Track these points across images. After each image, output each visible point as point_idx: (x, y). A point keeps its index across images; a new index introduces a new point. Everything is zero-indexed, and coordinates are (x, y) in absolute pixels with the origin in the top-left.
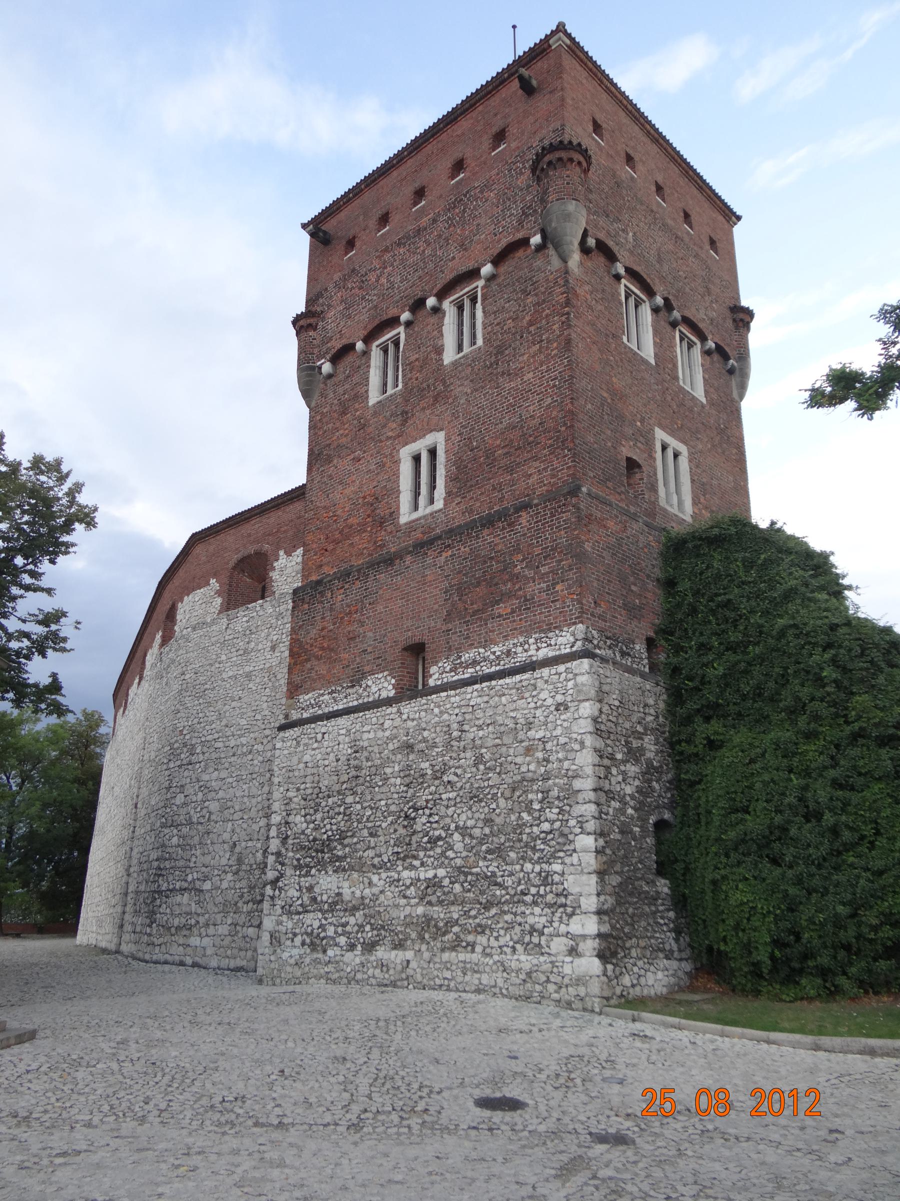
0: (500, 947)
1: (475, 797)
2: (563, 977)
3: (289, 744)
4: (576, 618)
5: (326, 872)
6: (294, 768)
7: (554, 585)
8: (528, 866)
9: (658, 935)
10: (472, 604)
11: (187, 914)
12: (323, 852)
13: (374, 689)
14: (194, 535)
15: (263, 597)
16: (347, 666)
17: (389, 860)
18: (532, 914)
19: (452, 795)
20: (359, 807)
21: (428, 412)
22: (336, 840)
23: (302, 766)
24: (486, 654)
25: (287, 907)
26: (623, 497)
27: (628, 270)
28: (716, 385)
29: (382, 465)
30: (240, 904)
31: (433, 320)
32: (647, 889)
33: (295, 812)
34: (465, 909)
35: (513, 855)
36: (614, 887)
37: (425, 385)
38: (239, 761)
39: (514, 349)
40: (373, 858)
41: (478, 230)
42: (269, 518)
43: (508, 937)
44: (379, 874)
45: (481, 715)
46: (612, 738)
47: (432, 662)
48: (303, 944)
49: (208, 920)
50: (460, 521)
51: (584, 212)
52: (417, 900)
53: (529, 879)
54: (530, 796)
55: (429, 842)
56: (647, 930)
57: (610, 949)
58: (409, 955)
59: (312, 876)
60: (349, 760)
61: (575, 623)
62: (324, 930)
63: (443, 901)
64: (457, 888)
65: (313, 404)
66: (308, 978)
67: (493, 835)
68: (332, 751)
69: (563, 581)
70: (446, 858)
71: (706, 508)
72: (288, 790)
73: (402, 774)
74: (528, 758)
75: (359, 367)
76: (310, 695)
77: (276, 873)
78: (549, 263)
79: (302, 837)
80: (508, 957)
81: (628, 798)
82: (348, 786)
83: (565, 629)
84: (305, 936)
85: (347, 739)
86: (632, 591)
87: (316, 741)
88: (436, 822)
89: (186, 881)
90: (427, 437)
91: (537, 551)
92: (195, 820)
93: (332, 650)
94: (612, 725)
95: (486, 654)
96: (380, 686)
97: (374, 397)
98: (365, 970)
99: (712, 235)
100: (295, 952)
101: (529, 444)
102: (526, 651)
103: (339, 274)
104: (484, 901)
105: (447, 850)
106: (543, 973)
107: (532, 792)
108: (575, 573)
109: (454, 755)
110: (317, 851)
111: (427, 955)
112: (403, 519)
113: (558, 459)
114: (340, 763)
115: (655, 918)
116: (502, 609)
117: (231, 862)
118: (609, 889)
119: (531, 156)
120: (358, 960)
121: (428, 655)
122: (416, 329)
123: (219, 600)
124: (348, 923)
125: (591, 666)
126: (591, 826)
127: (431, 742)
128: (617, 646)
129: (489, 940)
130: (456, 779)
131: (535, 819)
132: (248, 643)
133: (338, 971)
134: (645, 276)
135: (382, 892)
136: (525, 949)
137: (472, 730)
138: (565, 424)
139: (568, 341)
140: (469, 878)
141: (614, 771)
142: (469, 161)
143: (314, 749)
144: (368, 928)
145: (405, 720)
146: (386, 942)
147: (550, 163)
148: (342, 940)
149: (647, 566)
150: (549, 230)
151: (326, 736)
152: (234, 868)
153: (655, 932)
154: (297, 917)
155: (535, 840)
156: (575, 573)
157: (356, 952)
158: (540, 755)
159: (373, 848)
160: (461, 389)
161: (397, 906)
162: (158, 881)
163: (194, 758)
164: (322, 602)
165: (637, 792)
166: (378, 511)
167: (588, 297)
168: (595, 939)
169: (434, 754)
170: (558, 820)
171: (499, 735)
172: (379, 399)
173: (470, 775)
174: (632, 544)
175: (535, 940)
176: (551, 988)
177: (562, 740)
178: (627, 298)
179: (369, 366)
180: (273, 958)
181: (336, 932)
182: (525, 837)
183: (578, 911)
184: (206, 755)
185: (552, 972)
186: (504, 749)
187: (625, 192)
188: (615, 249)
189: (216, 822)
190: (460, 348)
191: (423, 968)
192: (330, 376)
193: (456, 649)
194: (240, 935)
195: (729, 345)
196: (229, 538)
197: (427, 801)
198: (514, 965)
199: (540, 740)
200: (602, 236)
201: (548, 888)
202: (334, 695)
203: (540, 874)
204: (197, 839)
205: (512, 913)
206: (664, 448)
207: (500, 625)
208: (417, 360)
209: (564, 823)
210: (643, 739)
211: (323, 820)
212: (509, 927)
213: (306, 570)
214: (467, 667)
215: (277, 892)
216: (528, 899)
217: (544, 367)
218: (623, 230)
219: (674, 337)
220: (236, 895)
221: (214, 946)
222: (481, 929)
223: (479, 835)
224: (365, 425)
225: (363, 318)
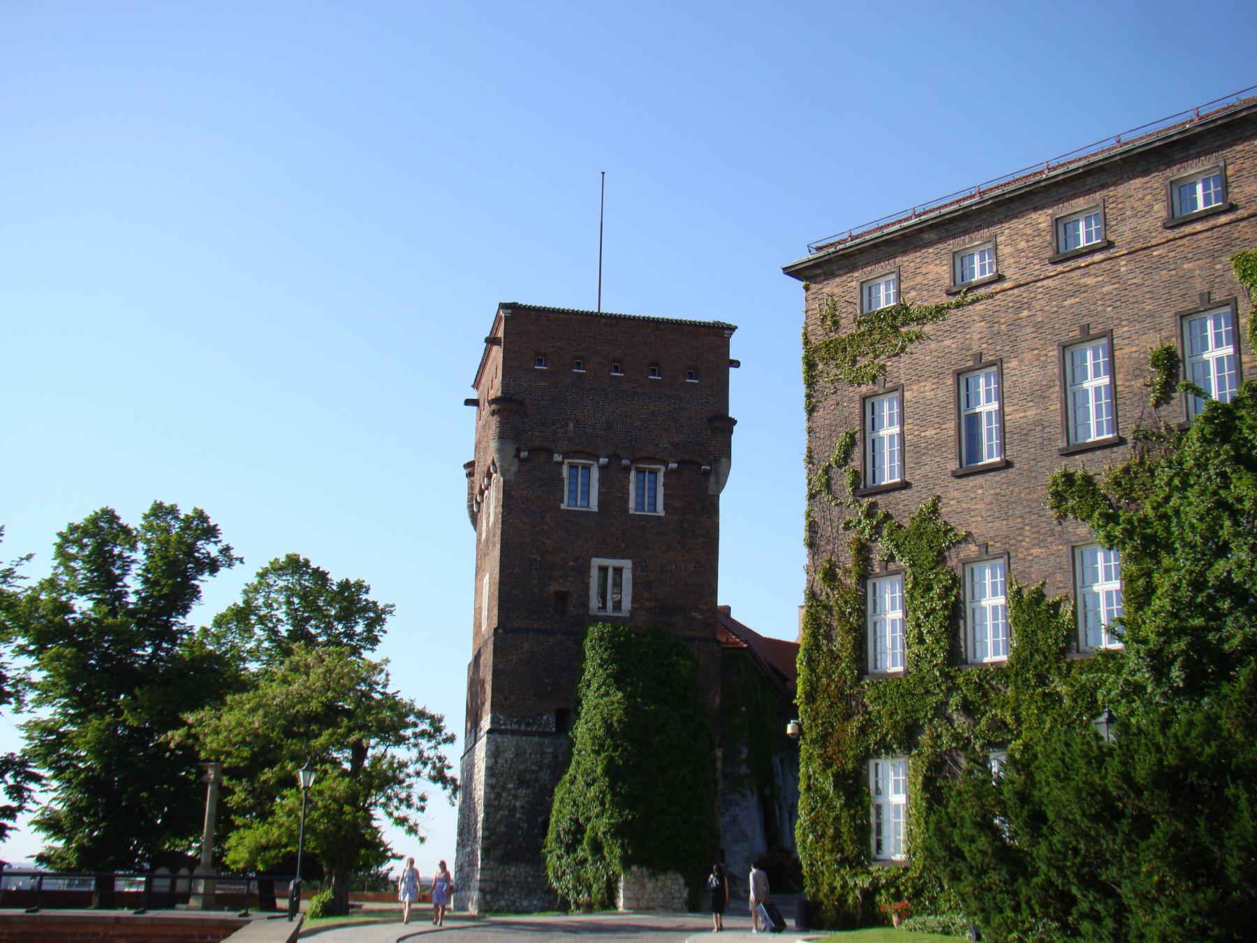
141: (504, 795)
200: (537, 443)
219: (628, 478)
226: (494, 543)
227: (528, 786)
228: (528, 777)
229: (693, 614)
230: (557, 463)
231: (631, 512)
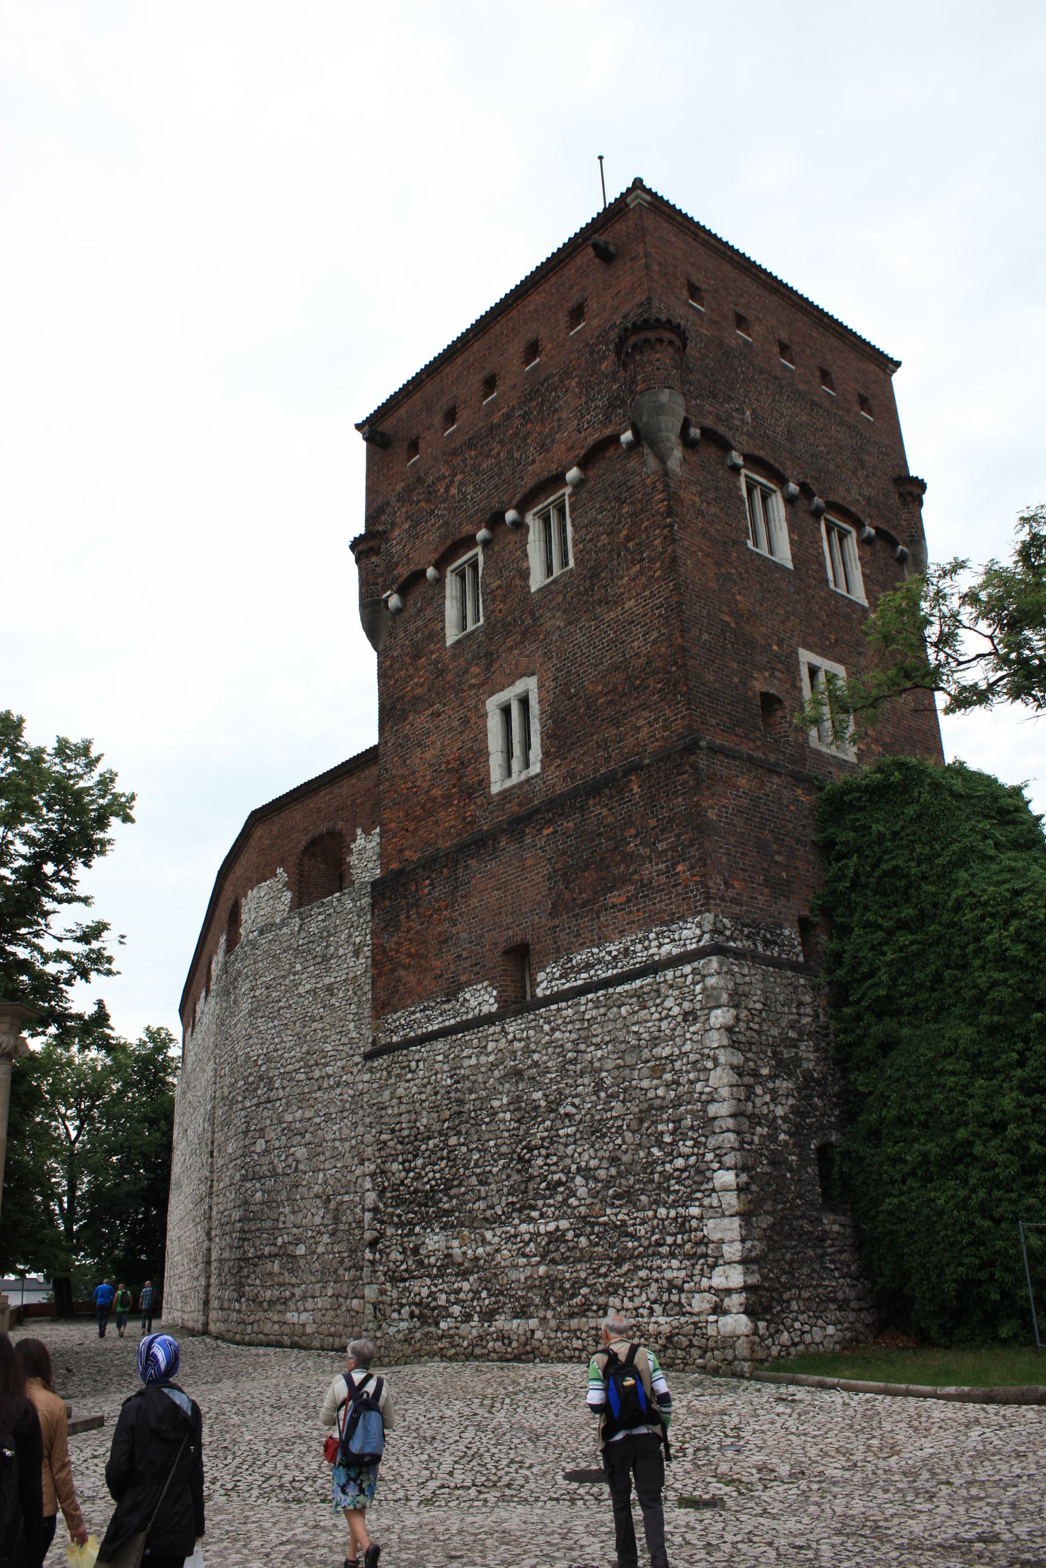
0: (636, 1309)
1: (596, 1131)
2: (708, 1340)
3: (378, 1075)
4: (701, 906)
5: (433, 1230)
6: (387, 1104)
7: (674, 865)
8: (662, 1212)
9: (827, 1283)
10: (581, 893)
11: (281, 1285)
12: (426, 1206)
13: (473, 1003)
14: (254, 814)
15: (340, 890)
16: (441, 976)
17: (503, 1212)
18: (670, 1268)
19: (571, 1130)
20: (464, 1149)
21: (516, 652)
22: (441, 1191)
23: (395, 1101)
24: (601, 955)
25: (390, 1273)
26: (759, 743)
27: (746, 457)
28: (881, 579)
29: (465, 722)
30: (340, 1272)
31: (514, 537)
32: (810, 1229)
33: (391, 1158)
34: (594, 1266)
35: (643, 1198)
36: (765, 1230)
37: (509, 619)
38: (326, 1097)
39: (611, 571)
40: (484, 1210)
41: (559, 426)
42: (341, 787)
43: (644, 1297)
44: (493, 1229)
45: (599, 1030)
46: (754, 1050)
47: (539, 968)
48: (412, 1315)
49: (305, 1292)
50: (561, 788)
51: (680, 400)
52: (538, 1259)
53: (664, 1227)
54: (660, 1127)
55: (547, 1188)
56: (813, 1278)
57: (761, 1303)
58: (533, 1323)
59: (416, 1235)
60: (449, 1093)
61: (700, 913)
62: (435, 1299)
63: (568, 1258)
64: (583, 1241)
65: (381, 647)
66: (421, 1356)
67: (621, 1177)
68: (429, 1083)
69: (683, 861)
70: (569, 1206)
71: (876, 741)
72: (381, 1132)
73: (512, 1108)
74: (655, 1082)
75: (432, 598)
76: (399, 1014)
77: (375, 1233)
78: (644, 463)
79: (402, 1188)
80: (645, 1320)
81: (780, 1122)
82: (451, 1125)
83: (690, 920)
84: (413, 1307)
85: (446, 1067)
86: (776, 862)
87: (410, 1071)
88: (555, 1164)
89: (275, 1245)
90: (517, 683)
91: (653, 822)
92: (280, 1170)
93: (420, 956)
94: (754, 1034)
95: (601, 955)
96: (480, 1000)
97: (452, 635)
98: (484, 1343)
99: (862, 392)
100: (404, 1325)
101: (636, 689)
102: (647, 949)
103: (402, 484)
104: (615, 1256)
105: (569, 1197)
106: (685, 1336)
107: (662, 1122)
108: (698, 849)
109: (570, 1081)
110: (420, 1205)
111: (553, 1323)
112: (495, 789)
113: (670, 707)
114: (439, 1097)
115: (822, 1263)
116: (616, 897)
117: (326, 1221)
118: (757, 1232)
119: (613, 336)
120: (475, 1332)
121: (535, 960)
122: (496, 549)
123: (288, 895)
124: (461, 1289)
125: (721, 965)
126: (729, 1160)
127: (543, 1066)
128: (758, 934)
129: (622, 1301)
130: (574, 1110)
131: (667, 1154)
132: (326, 947)
133: (454, 1347)
134: (772, 462)
135: (498, 1251)
136: (664, 1309)
137: (589, 1050)
138: (675, 663)
139: (674, 560)
140: (596, 1229)
141: (759, 1090)
142: (544, 342)
143: (408, 1081)
144: (484, 1294)
145: (512, 1041)
146: (506, 1310)
147: (635, 346)
148: (456, 1310)
149: (795, 828)
150: (640, 425)
151: (421, 1064)
152: (330, 1227)
153: (824, 1279)
154: (402, 1285)
155: (669, 1180)
156: (698, 849)
157: (472, 1324)
158: (668, 1077)
159: (485, 1198)
160: (553, 622)
161: (516, 1266)
162: (242, 1246)
163: (273, 1095)
164: (405, 897)
165: (792, 1113)
166: (465, 780)
167: (697, 499)
168: (741, 1292)
169: (547, 1081)
170: (693, 1154)
171: (620, 1054)
172: (457, 638)
173: (589, 1105)
174: (773, 802)
175: (675, 1298)
176: (695, 1352)
177: (693, 1057)
178: (750, 491)
179: (444, 596)
180: (378, 1334)
181: (448, 1301)
182: (656, 1176)
183: (721, 1262)
184: (288, 1089)
185: (695, 1335)
186: (627, 1071)
187: (736, 362)
188: (728, 435)
189: (305, 1173)
190: (549, 570)
191: (549, 1338)
192: (399, 611)
193: (566, 950)
194: (344, 1308)
195: (895, 528)
196: (296, 814)
197: (543, 1139)
198: (652, 1328)
199: (666, 1058)
200: (709, 422)
201: (686, 1237)
202: (427, 1012)
203: (675, 1219)
204: (284, 1193)
205: (647, 1268)
206: (813, 671)
207: (614, 918)
208: (499, 587)
209: (700, 1157)
210: (798, 1048)
211: (423, 1168)
212: (645, 1285)
213: (383, 856)
214: (579, 972)
215: (378, 1256)
216: (664, 1250)
217: (647, 593)
218: (737, 410)
219: (819, 530)
220: (335, 1261)
221: (314, 1322)
222: (612, 1289)
223: (604, 1177)
224: (443, 671)
225: (432, 538)
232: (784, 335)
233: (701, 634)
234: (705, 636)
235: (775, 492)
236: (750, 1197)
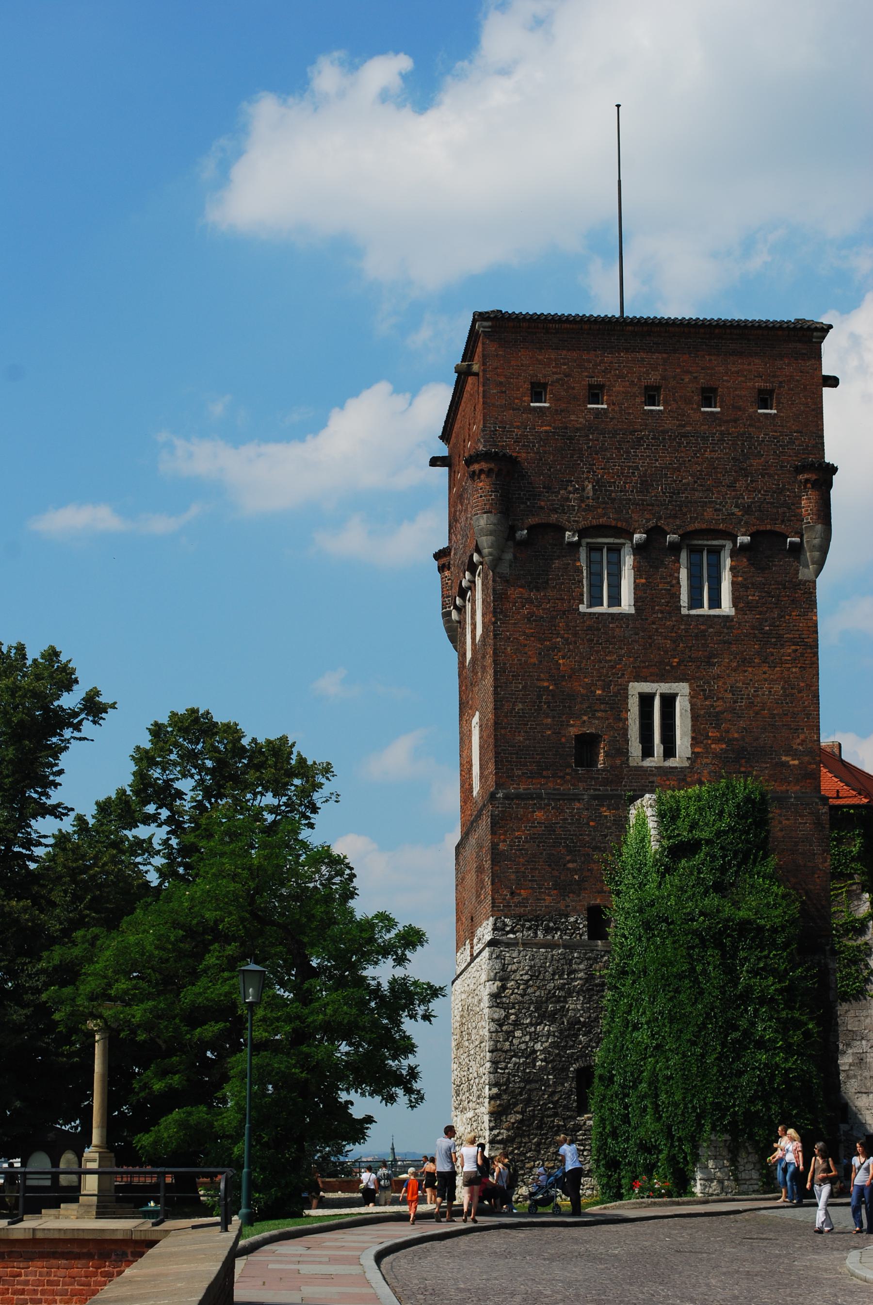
32: (561, 1123)
36: (513, 1123)
86: (568, 869)
118: (505, 1125)
219: (678, 561)
226: (484, 668)
227: (552, 1018)
228: (551, 1007)
229: (784, 758)
230: (571, 544)
231: (684, 611)
232: (654, 378)
233: (514, 705)
234: (520, 706)
235: (624, 544)
236: (498, 1102)
